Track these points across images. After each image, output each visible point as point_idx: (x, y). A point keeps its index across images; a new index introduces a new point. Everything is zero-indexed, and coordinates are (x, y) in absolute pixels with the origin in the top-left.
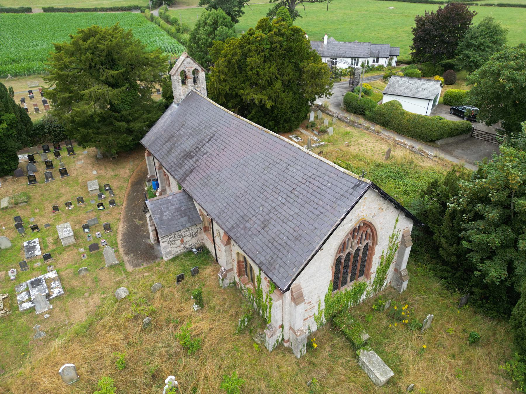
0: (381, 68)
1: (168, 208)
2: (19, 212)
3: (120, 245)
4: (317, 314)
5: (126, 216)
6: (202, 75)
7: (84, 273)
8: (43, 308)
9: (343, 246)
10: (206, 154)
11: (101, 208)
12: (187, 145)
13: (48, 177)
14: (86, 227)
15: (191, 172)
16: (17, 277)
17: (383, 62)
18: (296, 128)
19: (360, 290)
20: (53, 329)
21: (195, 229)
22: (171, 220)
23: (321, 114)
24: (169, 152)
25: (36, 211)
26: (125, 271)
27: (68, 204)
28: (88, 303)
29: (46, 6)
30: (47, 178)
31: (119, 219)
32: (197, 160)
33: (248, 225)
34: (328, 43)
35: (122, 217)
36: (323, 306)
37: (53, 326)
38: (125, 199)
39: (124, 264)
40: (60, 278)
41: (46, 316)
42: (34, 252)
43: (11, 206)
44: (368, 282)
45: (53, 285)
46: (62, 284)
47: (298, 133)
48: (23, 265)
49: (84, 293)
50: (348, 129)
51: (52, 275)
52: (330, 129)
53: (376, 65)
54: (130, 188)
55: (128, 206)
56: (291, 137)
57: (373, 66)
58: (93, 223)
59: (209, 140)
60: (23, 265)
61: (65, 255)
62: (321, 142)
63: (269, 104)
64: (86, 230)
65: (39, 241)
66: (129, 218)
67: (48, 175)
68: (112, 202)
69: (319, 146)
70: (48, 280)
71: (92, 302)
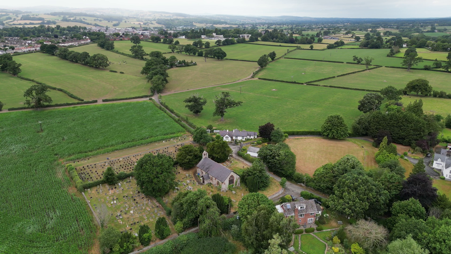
0: (251, 139)
6: (208, 154)
9: (230, 178)
12: (207, 167)
17: (252, 137)
19: (233, 185)
21: (209, 180)
23: (231, 157)
24: (204, 168)
27: (185, 178)
29: (104, 99)
34: (235, 132)
50: (237, 161)
52: (233, 161)
53: (250, 138)
57: (249, 138)
63: (219, 157)
66: (196, 180)
68: (192, 177)
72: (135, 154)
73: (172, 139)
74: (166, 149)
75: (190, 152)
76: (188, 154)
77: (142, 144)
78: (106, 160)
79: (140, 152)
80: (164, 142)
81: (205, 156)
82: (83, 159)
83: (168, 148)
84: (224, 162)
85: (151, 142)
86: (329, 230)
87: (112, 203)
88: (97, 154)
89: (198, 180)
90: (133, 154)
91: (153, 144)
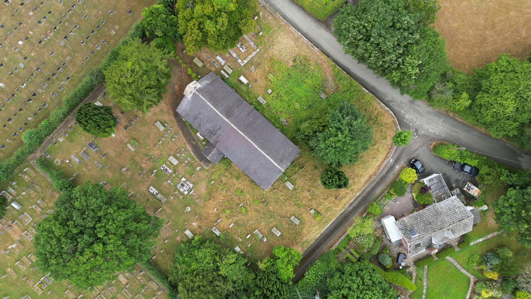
3: (195, 158)
5: (187, 141)
10: (221, 135)
12: (209, 126)
15: (217, 142)
31: (185, 143)
32: (218, 137)
33: (250, 171)
35: (185, 141)
38: (179, 129)
40: (187, 180)
42: (169, 172)
45: (188, 183)
49: (199, 182)
51: (183, 179)
54: (175, 119)
55: (183, 134)
56: (238, 46)
59: (219, 129)
61: (180, 168)
86: (481, 240)
89: (194, 140)
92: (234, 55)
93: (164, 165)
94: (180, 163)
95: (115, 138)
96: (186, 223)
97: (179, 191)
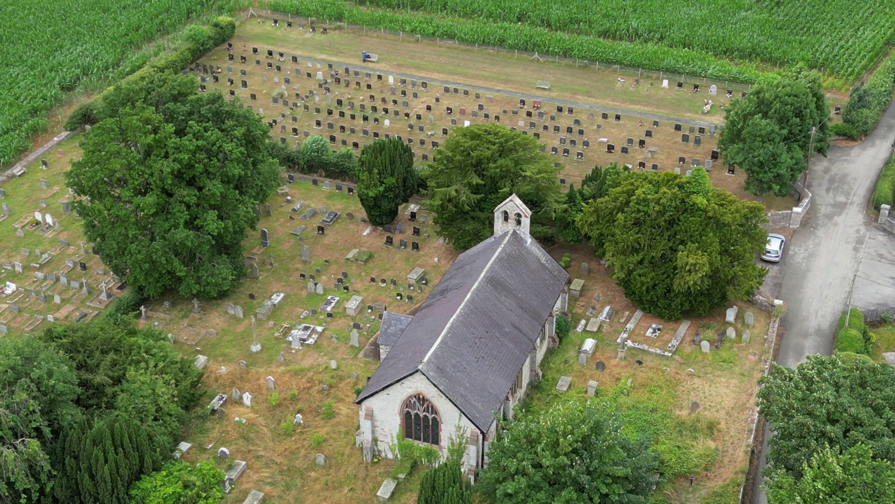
1: (396, 325)
2: (352, 269)
4: (391, 445)
7: (334, 340)
8: (296, 345)
9: (407, 404)
11: (399, 298)
13: (403, 244)
14: (370, 308)
16: (305, 318)
18: (670, 319)
20: (290, 361)
22: (393, 335)
25: (363, 274)
26: (357, 354)
27: (384, 281)
28: (318, 359)
30: (401, 245)
36: (396, 442)
37: (291, 359)
39: (361, 350)
40: (321, 334)
41: (294, 351)
43: (352, 259)
44: (441, 454)
45: (313, 336)
46: (318, 338)
47: (672, 325)
48: (314, 312)
51: (319, 329)
58: (378, 307)
60: (314, 312)
62: (670, 351)
64: (370, 311)
65: (338, 301)
67: (403, 243)
68: (410, 298)
69: (659, 355)
70: (314, 331)
71: (320, 359)
72: (480, 83)
73: (713, 88)
74: (605, 116)
75: (478, 167)
76: (462, 169)
77: (566, 53)
78: (358, 62)
79: (506, 82)
80: (665, 83)
81: (511, 226)
82: (312, 23)
83: (618, 118)
84: (661, 316)
85: (609, 62)
87: (38, 216)
88: (374, 24)
90: (469, 81)
91: (615, 71)
92: (630, 326)
93: (338, 298)
94: (353, 318)
95: (361, 236)
96: (220, 359)
97: (289, 329)
